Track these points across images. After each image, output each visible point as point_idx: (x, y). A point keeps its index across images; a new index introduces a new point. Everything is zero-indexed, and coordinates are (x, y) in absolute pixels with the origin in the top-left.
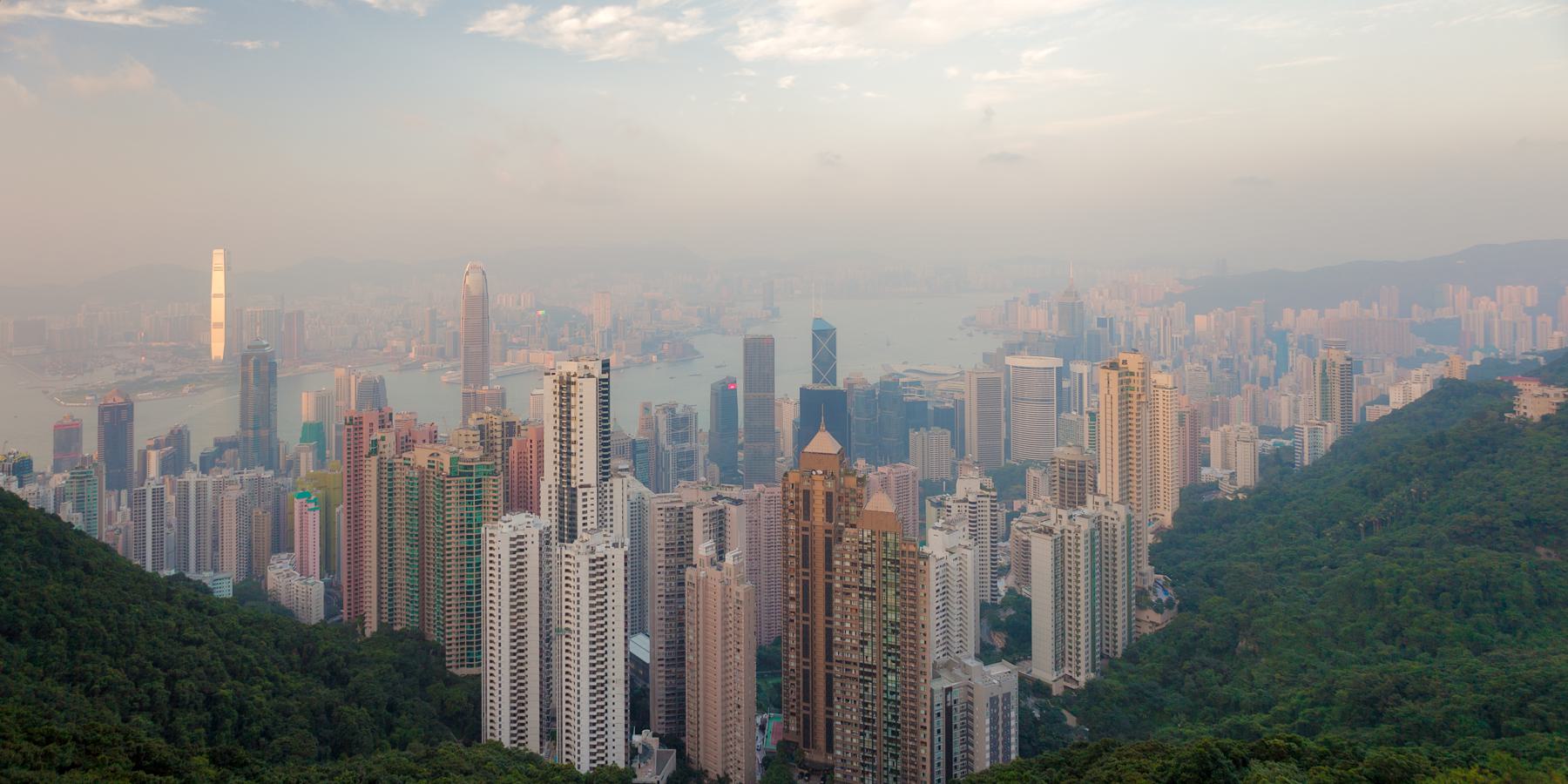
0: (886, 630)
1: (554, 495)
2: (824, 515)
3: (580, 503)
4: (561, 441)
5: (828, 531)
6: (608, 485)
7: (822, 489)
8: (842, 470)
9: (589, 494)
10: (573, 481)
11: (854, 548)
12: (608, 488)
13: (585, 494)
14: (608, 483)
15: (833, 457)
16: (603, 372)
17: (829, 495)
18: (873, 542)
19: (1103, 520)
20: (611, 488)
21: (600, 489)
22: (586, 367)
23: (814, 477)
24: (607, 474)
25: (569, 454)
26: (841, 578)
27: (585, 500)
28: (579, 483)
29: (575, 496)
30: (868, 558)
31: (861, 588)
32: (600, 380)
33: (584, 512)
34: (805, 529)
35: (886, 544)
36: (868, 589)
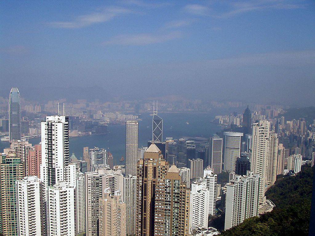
0: (174, 216)
1: (46, 171)
3: (56, 174)
5: (154, 182)
6: (68, 167)
8: (160, 159)
9: (60, 170)
10: (53, 165)
11: (163, 187)
12: (68, 169)
13: (58, 170)
14: (68, 167)
17: (155, 169)
24: (67, 163)
25: (52, 154)
27: (58, 173)
28: (56, 166)
29: (55, 171)
30: (168, 190)
31: (166, 201)
32: (64, 124)
33: (58, 177)
34: (146, 181)
35: (175, 184)
36: (167, 201)
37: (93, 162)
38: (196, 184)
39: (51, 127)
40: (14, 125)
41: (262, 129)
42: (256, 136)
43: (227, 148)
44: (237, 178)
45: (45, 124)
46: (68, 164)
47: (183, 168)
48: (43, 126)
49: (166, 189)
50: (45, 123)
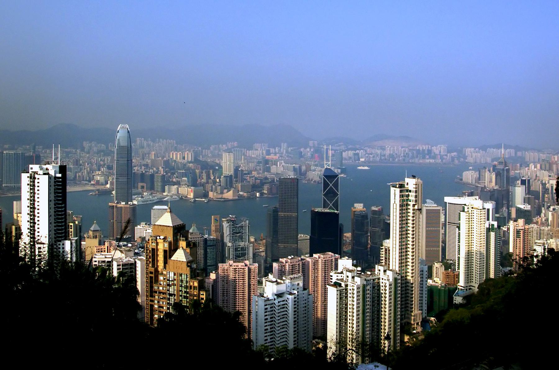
2: (163, 265)
4: (31, 215)
7: (162, 248)
11: (165, 283)
12: (61, 246)
13: (40, 248)
14: (61, 243)
15: (170, 228)
16: (60, 173)
17: (165, 251)
18: (174, 280)
19: (381, 281)
20: (63, 246)
21: (55, 246)
22: (47, 169)
23: (158, 241)
24: (61, 237)
26: (158, 302)
30: (171, 290)
34: (151, 273)
35: (182, 281)
37: (227, 240)
38: (273, 282)
39: (34, 182)
40: (121, 180)
41: (407, 193)
42: (395, 205)
43: (450, 223)
44: (348, 277)
45: (28, 177)
46: (61, 239)
47: (326, 254)
48: (25, 178)
49: (168, 287)
50: (28, 175)
